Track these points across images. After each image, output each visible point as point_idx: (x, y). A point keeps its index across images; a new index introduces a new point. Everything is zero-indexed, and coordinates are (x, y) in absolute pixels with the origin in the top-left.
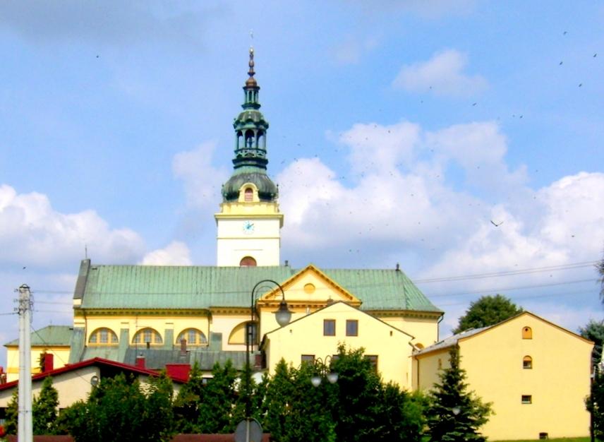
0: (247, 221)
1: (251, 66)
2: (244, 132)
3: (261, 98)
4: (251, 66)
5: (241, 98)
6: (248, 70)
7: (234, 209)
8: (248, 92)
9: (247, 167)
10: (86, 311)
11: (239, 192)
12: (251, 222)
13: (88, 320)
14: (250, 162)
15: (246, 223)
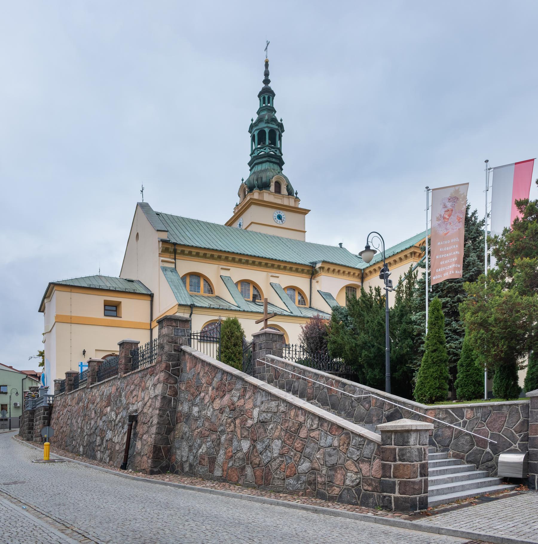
0: (278, 211)
1: (267, 74)
2: (267, 131)
3: (277, 103)
4: (267, 74)
5: (256, 104)
6: (263, 78)
7: (268, 197)
8: (266, 97)
9: (271, 164)
10: (177, 248)
11: (270, 183)
12: (282, 213)
13: (178, 261)
14: (274, 160)
15: (276, 213)
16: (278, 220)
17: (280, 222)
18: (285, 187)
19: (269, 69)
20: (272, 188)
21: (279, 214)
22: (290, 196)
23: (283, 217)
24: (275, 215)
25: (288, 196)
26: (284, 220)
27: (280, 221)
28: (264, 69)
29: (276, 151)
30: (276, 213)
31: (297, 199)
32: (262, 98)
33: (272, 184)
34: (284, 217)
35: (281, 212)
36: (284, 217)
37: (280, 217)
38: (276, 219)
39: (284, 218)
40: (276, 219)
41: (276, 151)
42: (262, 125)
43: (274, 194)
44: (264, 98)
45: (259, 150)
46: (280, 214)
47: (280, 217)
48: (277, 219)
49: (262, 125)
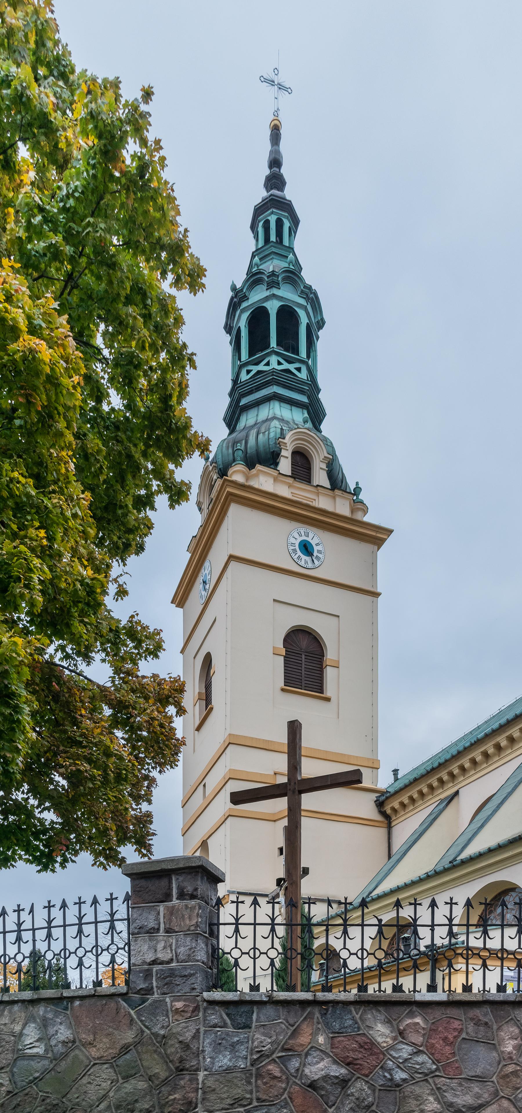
1: (275, 163)
4: (275, 163)
6: (267, 172)
16: (304, 557)
17: (306, 562)
18: (324, 466)
19: (284, 146)
20: (285, 465)
21: (304, 538)
22: (337, 492)
23: (316, 548)
24: (292, 540)
25: (330, 493)
26: (318, 558)
27: (308, 559)
28: (267, 146)
29: (299, 370)
30: (296, 535)
31: (359, 506)
32: (260, 230)
33: (283, 453)
34: (320, 548)
35: (311, 535)
36: (320, 548)
37: (306, 548)
38: (295, 551)
39: (319, 552)
40: (295, 551)
41: (299, 370)
42: (257, 295)
43: (291, 480)
44: (267, 224)
45: (250, 367)
46: (309, 539)
47: (306, 548)
48: (299, 553)
49: (257, 295)
